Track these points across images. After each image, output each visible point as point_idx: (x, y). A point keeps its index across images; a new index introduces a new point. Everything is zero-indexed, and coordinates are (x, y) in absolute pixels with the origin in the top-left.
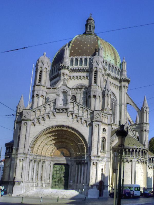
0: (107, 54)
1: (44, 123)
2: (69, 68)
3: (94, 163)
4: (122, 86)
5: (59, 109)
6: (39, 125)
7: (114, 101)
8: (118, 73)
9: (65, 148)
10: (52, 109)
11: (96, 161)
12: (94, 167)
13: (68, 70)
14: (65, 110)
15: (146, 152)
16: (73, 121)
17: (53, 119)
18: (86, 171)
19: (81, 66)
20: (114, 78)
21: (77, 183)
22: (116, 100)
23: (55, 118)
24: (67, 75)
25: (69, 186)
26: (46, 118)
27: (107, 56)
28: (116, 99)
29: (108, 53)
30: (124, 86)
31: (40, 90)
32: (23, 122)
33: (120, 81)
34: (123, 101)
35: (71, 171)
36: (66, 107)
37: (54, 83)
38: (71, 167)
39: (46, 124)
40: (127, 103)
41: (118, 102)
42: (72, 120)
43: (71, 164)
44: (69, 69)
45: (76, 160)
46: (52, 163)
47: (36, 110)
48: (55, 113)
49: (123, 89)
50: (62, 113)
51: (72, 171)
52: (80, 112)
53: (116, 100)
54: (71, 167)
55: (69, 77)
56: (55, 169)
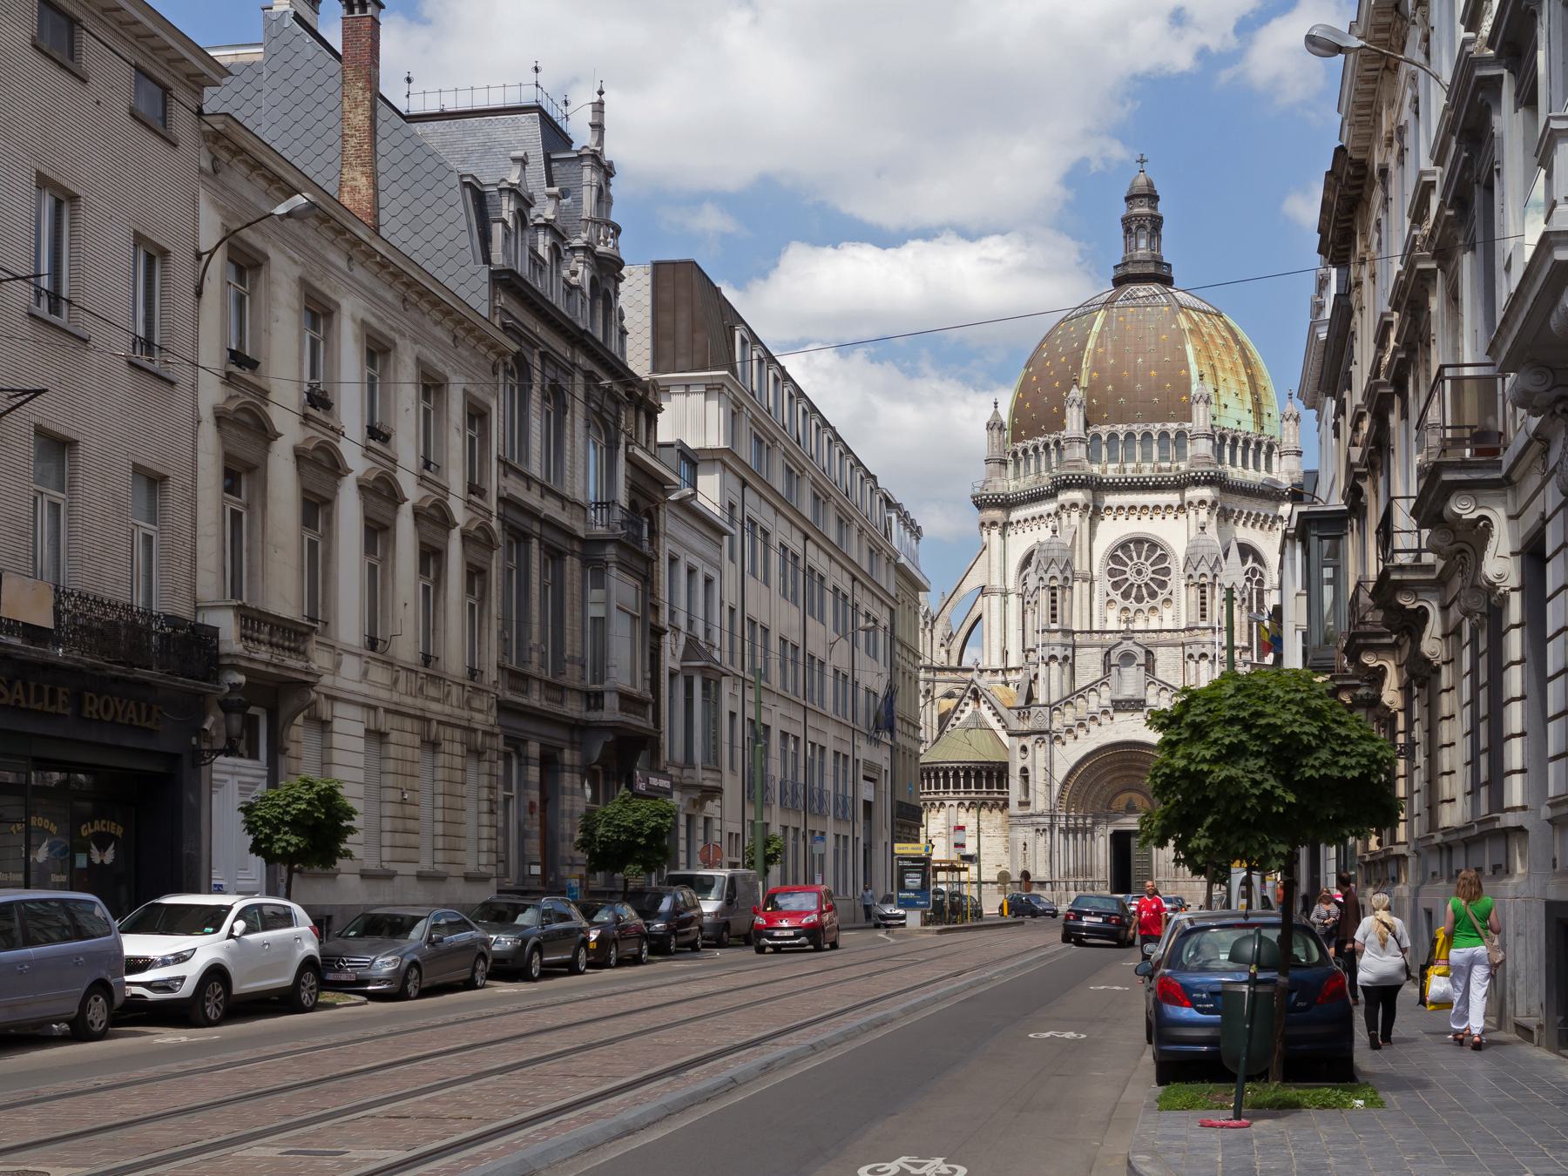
0: (1222, 403)
9: (1137, 791)
27: (1226, 406)
29: (1229, 389)
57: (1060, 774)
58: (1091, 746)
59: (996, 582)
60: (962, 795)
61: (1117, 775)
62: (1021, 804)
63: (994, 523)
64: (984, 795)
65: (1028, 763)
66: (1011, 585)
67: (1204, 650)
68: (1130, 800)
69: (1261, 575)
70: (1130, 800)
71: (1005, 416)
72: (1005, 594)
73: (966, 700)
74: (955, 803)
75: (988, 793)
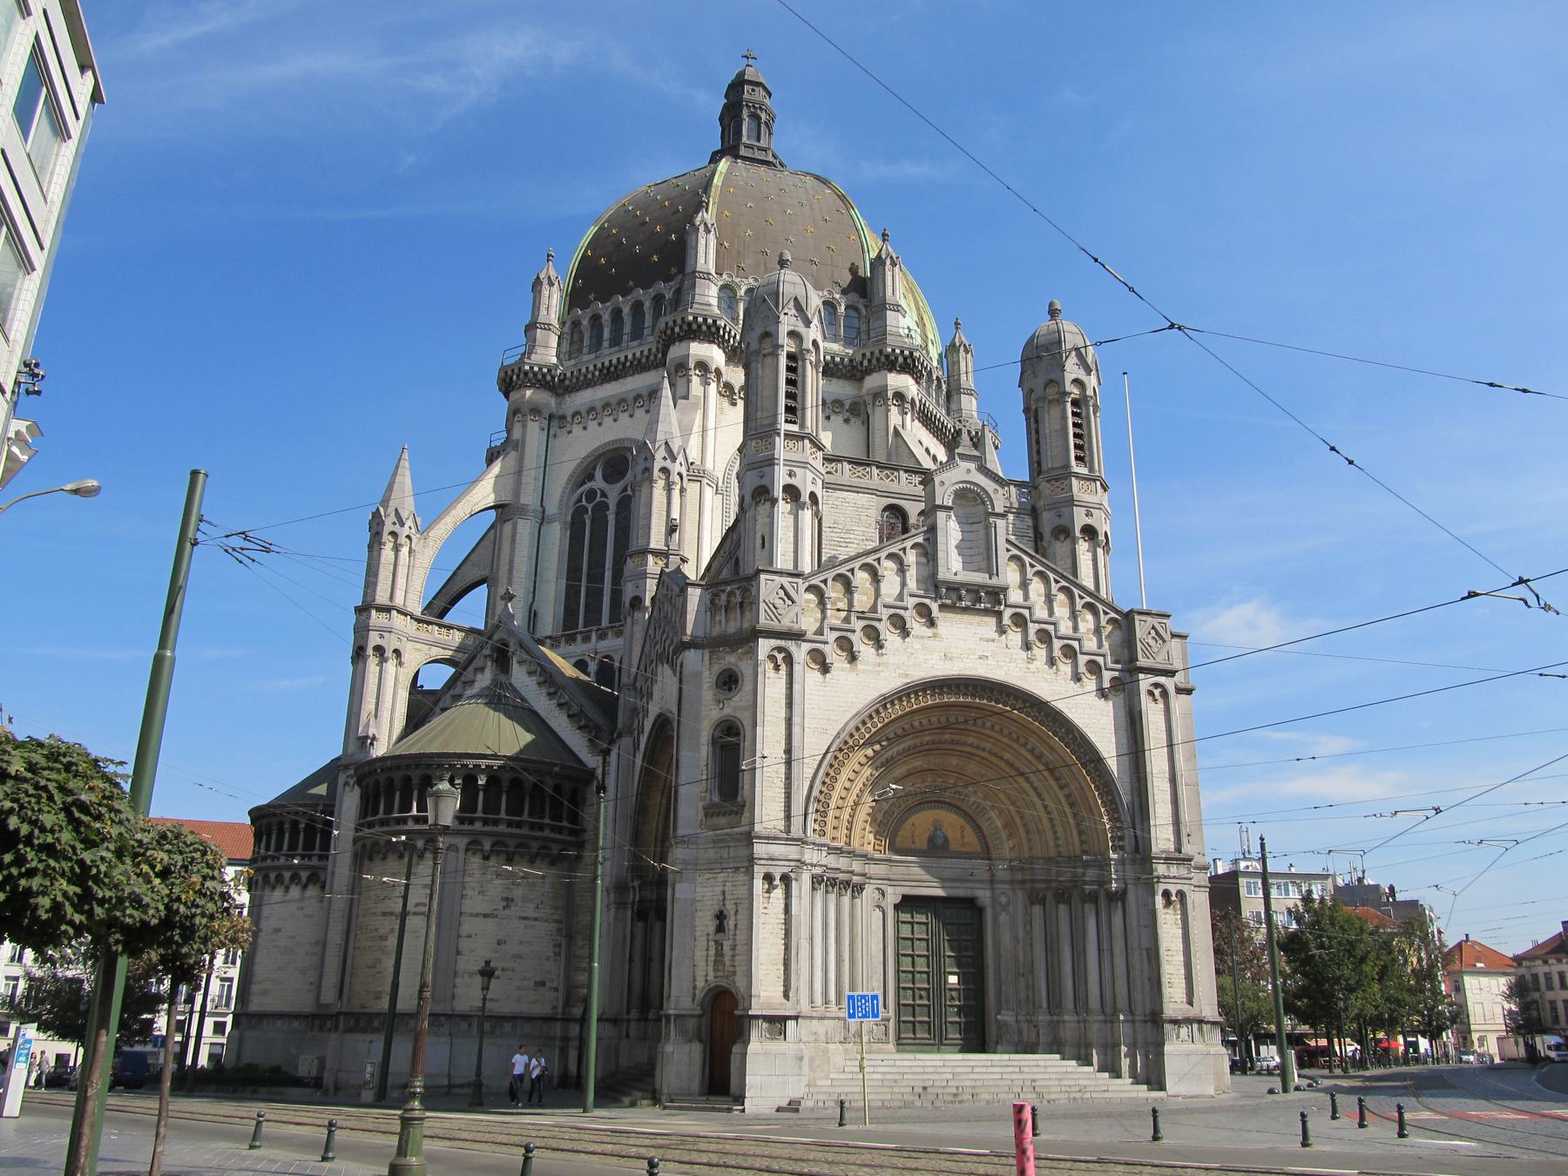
1: (878, 660)
3: (1166, 894)
5: (977, 592)
6: (851, 670)
10: (912, 584)
11: (1179, 887)
12: (1168, 917)
13: (721, 351)
14: (985, 600)
16: (1031, 660)
17: (925, 641)
18: (1119, 945)
21: (1055, 1005)
23: (935, 635)
25: (992, 1031)
26: (890, 637)
31: (804, 465)
32: (765, 646)
35: (997, 942)
36: (994, 581)
37: (606, 406)
38: (995, 917)
39: (886, 664)
42: (1024, 654)
43: (994, 898)
45: (1023, 882)
46: (893, 896)
47: (825, 581)
48: (934, 607)
50: (966, 610)
51: (1006, 939)
52: (1062, 611)
54: (995, 917)
56: (906, 931)
57: (814, 742)
58: (890, 682)
59: (529, 498)
60: (478, 826)
61: (917, 763)
62: (710, 811)
63: (535, 411)
64: (525, 831)
65: (735, 706)
66: (552, 508)
67: (1089, 521)
68: (937, 826)
70: (937, 826)
72: (543, 519)
73: (478, 662)
74: (462, 842)
75: (532, 826)
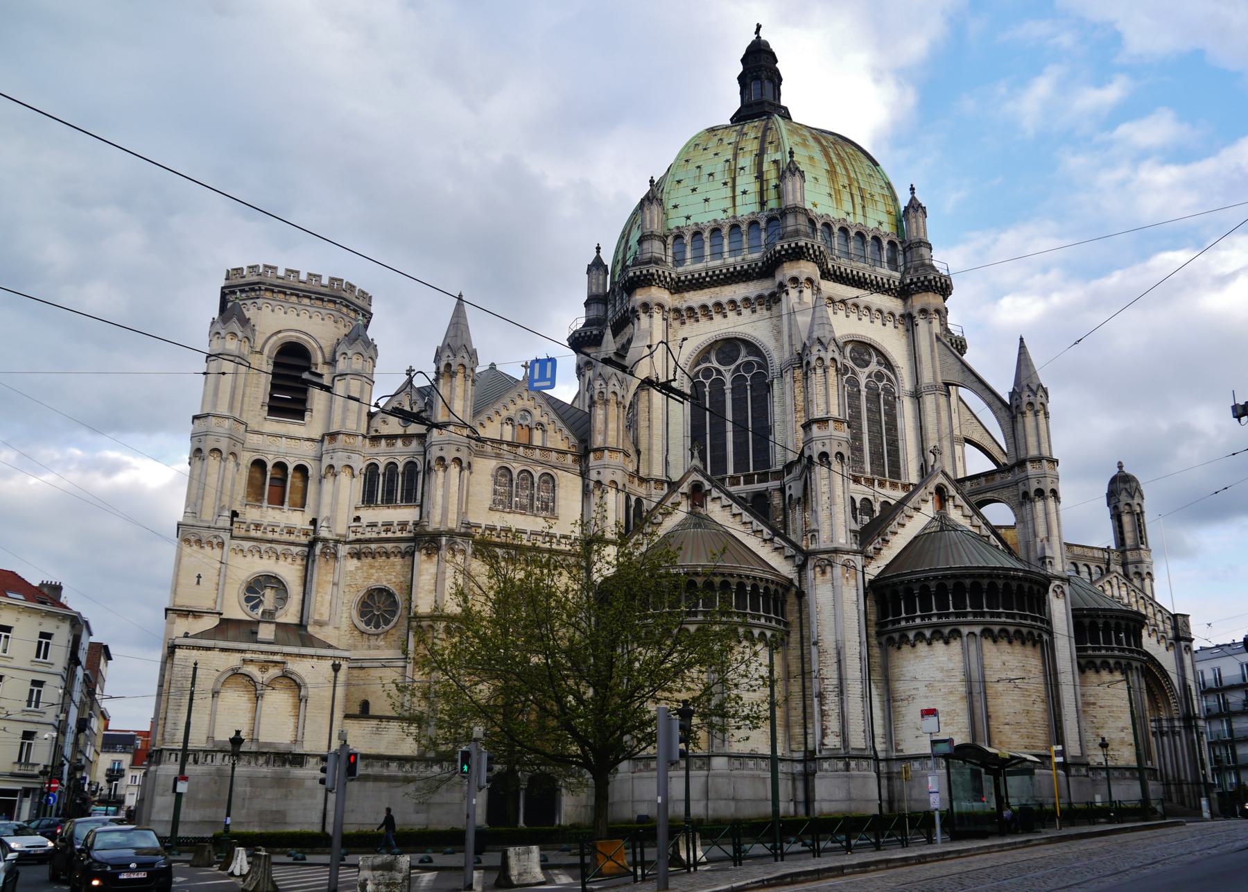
2: (665, 278)
4: (915, 314)
7: (885, 382)
8: (888, 262)
15: (1038, 590)
19: (718, 263)
20: (873, 285)
22: (892, 377)
24: (661, 306)
28: (894, 373)
30: (924, 311)
33: (903, 292)
34: (927, 377)
40: (945, 384)
41: (907, 384)
44: (668, 279)
49: (922, 325)
53: (892, 377)
55: (672, 314)
69: (889, 380)
71: (608, 259)
